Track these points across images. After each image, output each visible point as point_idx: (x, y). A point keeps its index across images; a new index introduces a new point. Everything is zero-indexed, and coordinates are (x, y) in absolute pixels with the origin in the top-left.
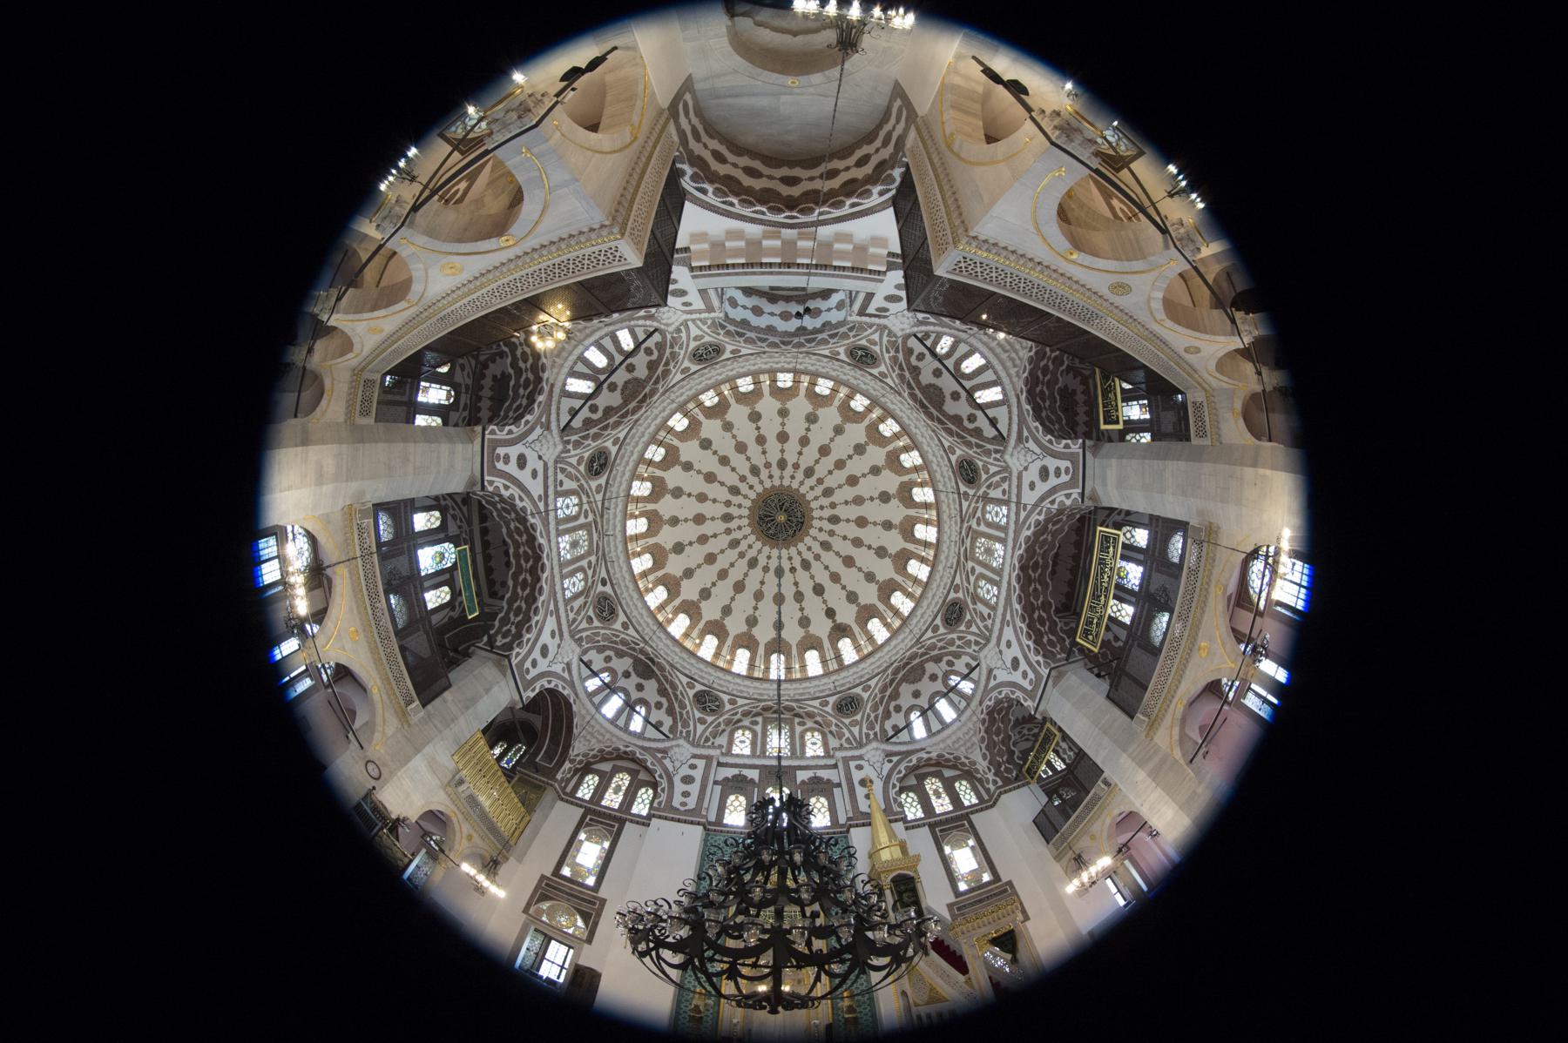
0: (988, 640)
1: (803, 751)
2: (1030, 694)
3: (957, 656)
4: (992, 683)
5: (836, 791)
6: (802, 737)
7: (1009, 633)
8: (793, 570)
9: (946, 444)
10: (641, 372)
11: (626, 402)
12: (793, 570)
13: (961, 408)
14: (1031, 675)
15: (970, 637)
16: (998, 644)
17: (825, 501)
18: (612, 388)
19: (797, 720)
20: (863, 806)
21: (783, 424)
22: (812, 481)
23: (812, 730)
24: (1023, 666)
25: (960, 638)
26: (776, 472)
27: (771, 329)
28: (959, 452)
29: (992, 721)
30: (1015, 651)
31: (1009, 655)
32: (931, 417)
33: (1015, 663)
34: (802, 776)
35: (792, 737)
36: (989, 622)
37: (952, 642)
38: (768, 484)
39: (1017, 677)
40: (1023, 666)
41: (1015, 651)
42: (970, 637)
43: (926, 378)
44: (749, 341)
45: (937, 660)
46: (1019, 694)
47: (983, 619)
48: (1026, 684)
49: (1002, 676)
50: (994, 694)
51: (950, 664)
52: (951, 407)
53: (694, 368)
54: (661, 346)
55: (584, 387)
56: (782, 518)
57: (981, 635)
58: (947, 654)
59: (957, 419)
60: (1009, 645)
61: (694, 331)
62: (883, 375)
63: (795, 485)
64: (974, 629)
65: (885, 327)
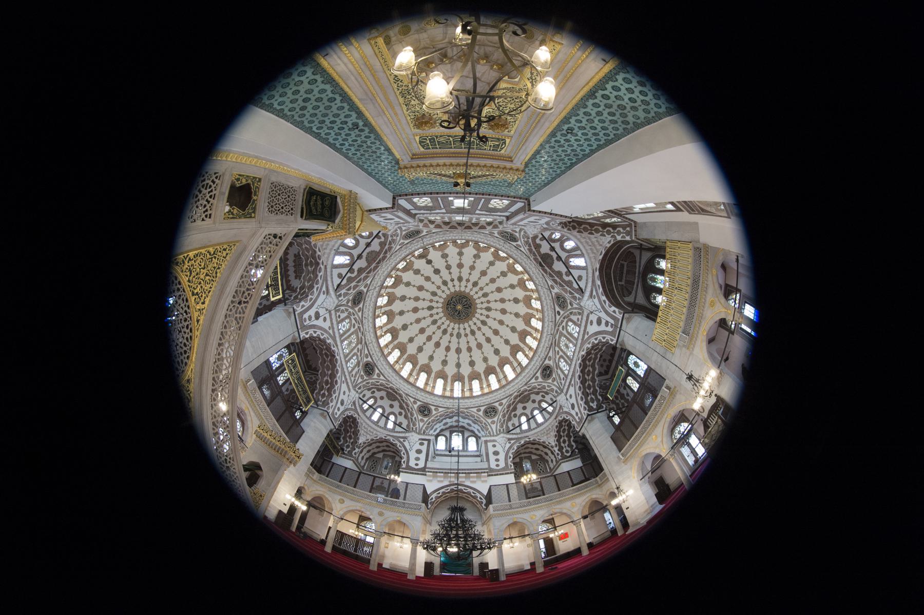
8: (452, 280)
9: (382, 377)
10: (520, 406)
11: (529, 395)
12: (452, 280)
13: (378, 394)
17: (436, 317)
18: (534, 401)
21: (458, 358)
22: (443, 327)
26: (462, 332)
27: (464, 418)
28: (375, 377)
32: (391, 388)
38: (466, 325)
43: (396, 404)
44: (474, 417)
52: (383, 394)
53: (497, 404)
54: (510, 419)
55: (544, 405)
56: (459, 307)
59: (379, 390)
61: (494, 426)
62: (415, 403)
63: (452, 324)
65: (419, 434)
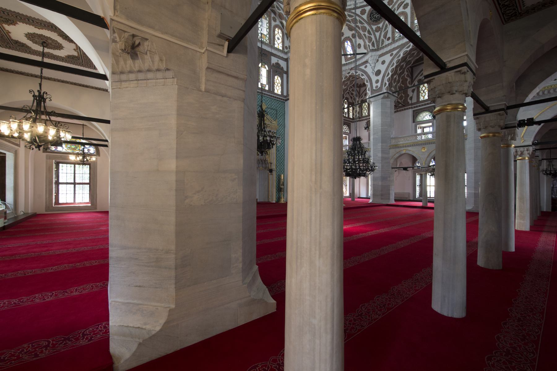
0: (378, 50)
1: (274, 44)
2: (373, 91)
3: (360, 37)
4: (363, 67)
5: (285, 76)
6: (274, 31)
7: (388, 58)
14: (379, 85)
15: (373, 37)
16: (380, 56)
19: (273, 15)
23: (279, 28)
24: (380, 78)
25: (369, 32)
29: (349, 79)
30: (383, 68)
31: (379, 66)
33: (378, 73)
34: (274, 60)
35: (270, 28)
36: (386, 42)
37: (364, 29)
39: (374, 78)
40: (380, 78)
41: (383, 68)
42: (373, 37)
45: (351, 29)
46: (368, 84)
47: (385, 36)
48: (374, 85)
49: (369, 70)
50: (359, 72)
51: (354, 36)
57: (378, 42)
58: (356, 31)
60: (383, 62)
64: (377, 34)
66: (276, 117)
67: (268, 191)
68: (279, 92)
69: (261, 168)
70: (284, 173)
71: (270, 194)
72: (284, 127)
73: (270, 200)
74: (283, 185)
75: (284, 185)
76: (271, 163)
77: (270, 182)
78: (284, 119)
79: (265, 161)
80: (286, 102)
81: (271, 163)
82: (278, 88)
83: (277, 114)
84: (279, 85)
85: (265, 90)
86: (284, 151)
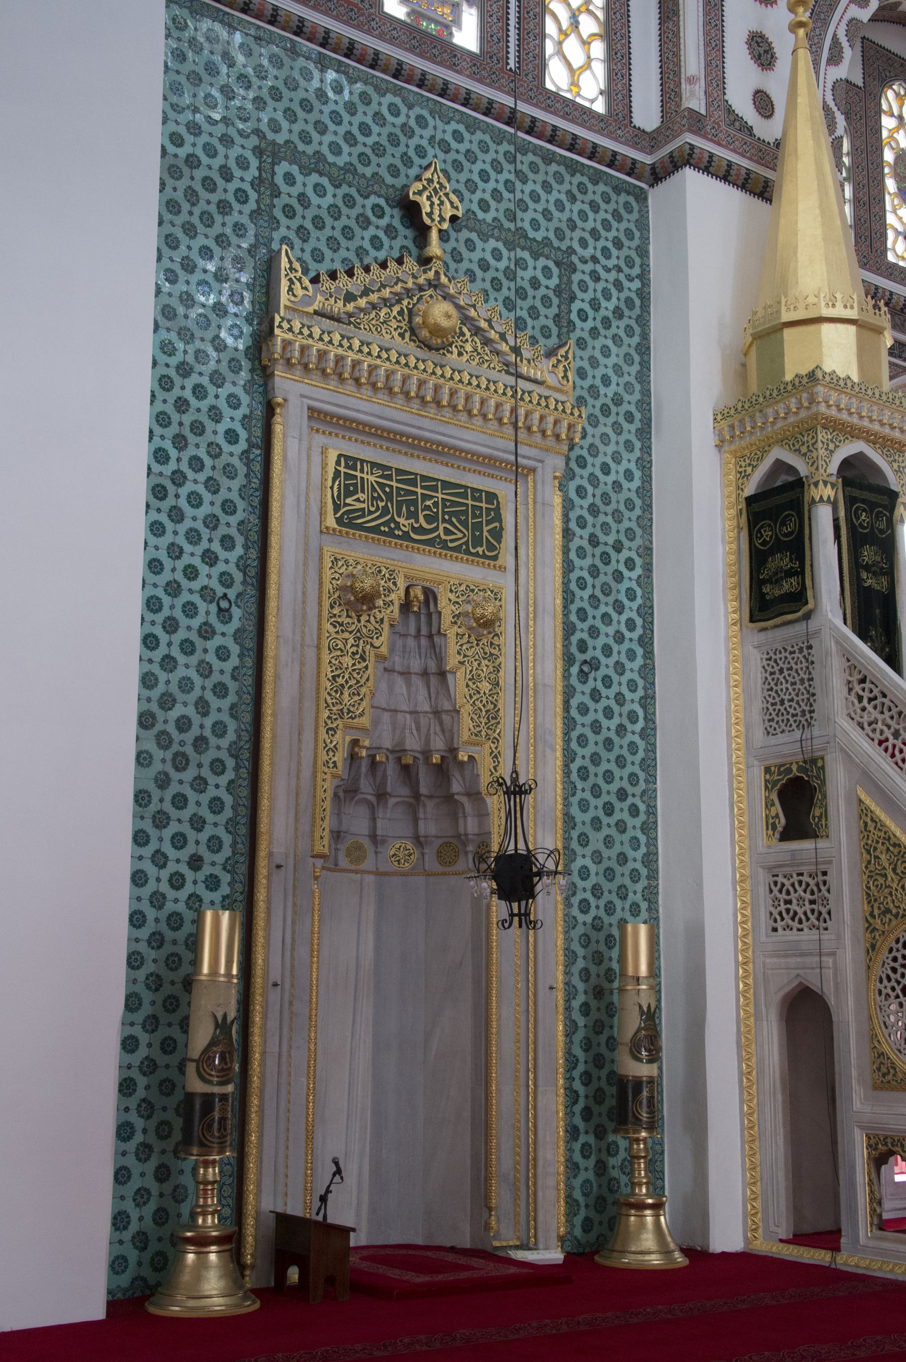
20: (740, 100)
66: (564, 323)
67: (482, 1127)
68: (591, 91)
69: (399, 846)
70: (649, 907)
71: (504, 1157)
72: (645, 433)
73: (504, 1236)
74: (649, 1042)
75: (654, 1057)
76: (516, 791)
77: (506, 1015)
78: (644, 349)
79: (442, 771)
80: (656, 196)
81: (516, 791)
82: (573, 49)
83: (565, 293)
84: (588, 26)
85: (452, 55)
86: (648, 670)
